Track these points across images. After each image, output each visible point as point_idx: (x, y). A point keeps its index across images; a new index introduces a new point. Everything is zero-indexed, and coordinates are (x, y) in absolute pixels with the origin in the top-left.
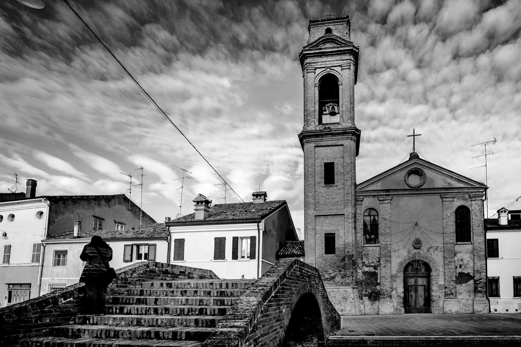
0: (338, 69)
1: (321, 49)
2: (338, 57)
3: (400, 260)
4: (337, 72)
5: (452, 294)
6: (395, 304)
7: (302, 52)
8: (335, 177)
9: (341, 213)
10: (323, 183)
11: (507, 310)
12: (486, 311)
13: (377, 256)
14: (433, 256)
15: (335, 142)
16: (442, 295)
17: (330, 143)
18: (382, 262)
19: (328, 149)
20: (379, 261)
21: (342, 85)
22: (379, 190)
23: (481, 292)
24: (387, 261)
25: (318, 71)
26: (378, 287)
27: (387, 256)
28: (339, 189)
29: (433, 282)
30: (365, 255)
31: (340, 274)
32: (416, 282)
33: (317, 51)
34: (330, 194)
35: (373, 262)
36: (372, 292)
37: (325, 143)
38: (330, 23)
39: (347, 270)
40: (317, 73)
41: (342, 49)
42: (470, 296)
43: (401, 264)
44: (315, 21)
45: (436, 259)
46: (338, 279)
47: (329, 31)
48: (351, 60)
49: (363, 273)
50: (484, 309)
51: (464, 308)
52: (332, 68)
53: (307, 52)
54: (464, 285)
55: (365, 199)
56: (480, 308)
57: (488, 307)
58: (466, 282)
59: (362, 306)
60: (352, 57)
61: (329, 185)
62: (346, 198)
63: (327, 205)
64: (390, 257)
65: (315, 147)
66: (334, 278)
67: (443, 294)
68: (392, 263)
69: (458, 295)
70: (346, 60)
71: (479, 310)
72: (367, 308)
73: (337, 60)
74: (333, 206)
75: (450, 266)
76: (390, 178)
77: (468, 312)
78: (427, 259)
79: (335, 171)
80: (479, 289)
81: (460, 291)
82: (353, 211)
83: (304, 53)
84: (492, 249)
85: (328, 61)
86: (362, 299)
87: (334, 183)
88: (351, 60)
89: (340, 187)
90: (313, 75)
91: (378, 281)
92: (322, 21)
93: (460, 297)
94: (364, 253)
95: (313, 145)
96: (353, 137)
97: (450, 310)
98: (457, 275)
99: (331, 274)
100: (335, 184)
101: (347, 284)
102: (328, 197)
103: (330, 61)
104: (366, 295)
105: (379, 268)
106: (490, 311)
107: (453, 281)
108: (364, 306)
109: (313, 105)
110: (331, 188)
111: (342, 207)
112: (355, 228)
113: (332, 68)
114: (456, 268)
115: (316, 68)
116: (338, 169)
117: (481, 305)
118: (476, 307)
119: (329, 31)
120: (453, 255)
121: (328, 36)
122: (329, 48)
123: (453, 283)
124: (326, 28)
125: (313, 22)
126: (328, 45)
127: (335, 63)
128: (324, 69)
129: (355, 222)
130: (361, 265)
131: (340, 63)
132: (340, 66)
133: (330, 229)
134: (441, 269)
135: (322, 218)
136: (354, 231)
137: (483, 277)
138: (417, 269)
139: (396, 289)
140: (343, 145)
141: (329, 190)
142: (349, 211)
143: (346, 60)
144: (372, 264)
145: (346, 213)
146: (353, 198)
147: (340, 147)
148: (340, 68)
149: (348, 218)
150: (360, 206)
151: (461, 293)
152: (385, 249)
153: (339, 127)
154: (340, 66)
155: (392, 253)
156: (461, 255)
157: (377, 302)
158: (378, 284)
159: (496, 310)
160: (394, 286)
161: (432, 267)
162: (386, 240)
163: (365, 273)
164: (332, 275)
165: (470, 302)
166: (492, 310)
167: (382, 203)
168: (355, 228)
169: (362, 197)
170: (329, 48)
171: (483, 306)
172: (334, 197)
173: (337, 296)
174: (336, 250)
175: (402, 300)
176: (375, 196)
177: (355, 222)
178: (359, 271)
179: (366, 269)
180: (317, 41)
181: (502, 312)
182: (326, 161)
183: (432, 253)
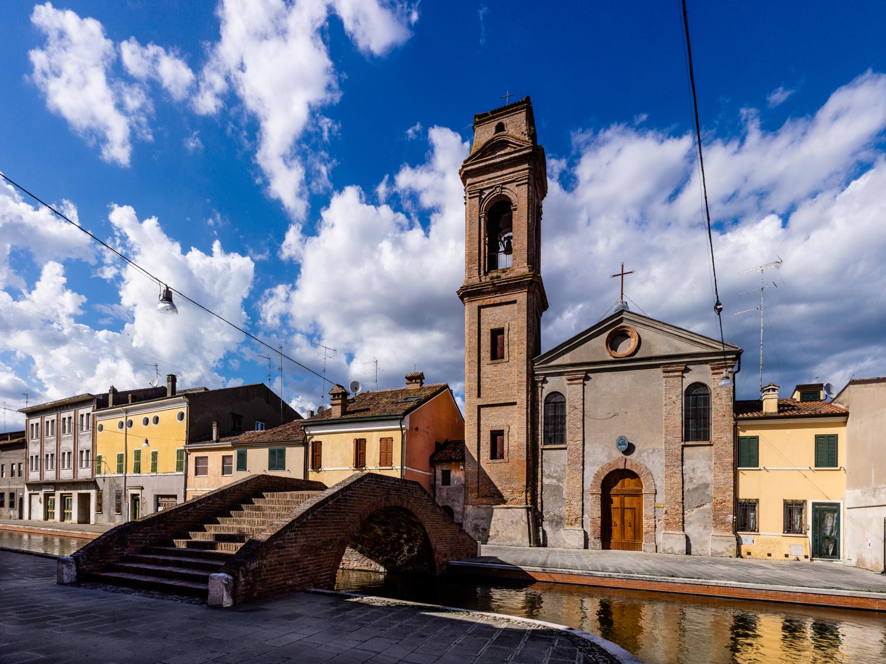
0: (512, 186)
3: (596, 469)
7: (463, 167)
9: (512, 401)
17: (498, 300)
21: (515, 209)
28: (510, 366)
32: (622, 502)
38: (502, 115)
40: (483, 197)
43: (597, 475)
47: (500, 128)
55: (548, 379)
75: (673, 480)
87: (503, 357)
100: (506, 359)
119: (500, 128)
124: (496, 123)
127: (507, 178)
135: (488, 409)
138: (618, 487)
140: (515, 302)
142: (522, 397)
145: (518, 401)
153: (511, 275)
170: (502, 156)
182: (493, 326)
183: (646, 459)
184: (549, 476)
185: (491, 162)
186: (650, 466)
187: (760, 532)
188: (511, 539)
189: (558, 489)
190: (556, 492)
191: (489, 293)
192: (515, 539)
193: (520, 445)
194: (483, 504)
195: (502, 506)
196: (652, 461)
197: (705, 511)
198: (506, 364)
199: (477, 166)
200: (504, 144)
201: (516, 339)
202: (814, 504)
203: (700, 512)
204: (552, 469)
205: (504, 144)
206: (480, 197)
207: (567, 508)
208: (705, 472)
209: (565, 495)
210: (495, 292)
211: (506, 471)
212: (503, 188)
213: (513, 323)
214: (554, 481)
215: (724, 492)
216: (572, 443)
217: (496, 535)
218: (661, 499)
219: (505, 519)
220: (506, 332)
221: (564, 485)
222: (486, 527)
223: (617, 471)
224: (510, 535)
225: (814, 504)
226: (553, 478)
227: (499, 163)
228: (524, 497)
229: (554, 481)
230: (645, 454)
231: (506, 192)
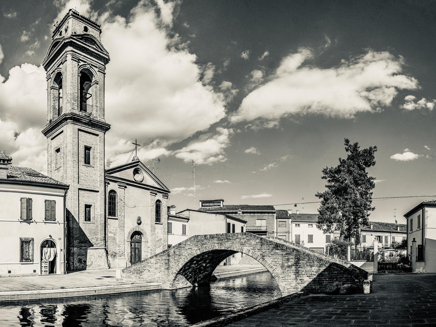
0: (97, 70)
35: (113, 230)
127: (94, 63)
184: (111, 232)
186: (145, 230)
188: (99, 266)
189: (114, 239)
190: (114, 240)
191: (85, 124)
192: (101, 266)
194: (82, 247)
195: (91, 248)
196: (145, 228)
206: (78, 65)
207: (118, 248)
209: (117, 242)
210: (89, 125)
211: (94, 228)
214: (112, 235)
217: (91, 264)
219: (95, 255)
221: (117, 237)
222: (85, 260)
223: (136, 231)
224: (99, 263)
226: (112, 233)
227: (91, 51)
228: (103, 243)
229: (112, 235)
230: (144, 225)
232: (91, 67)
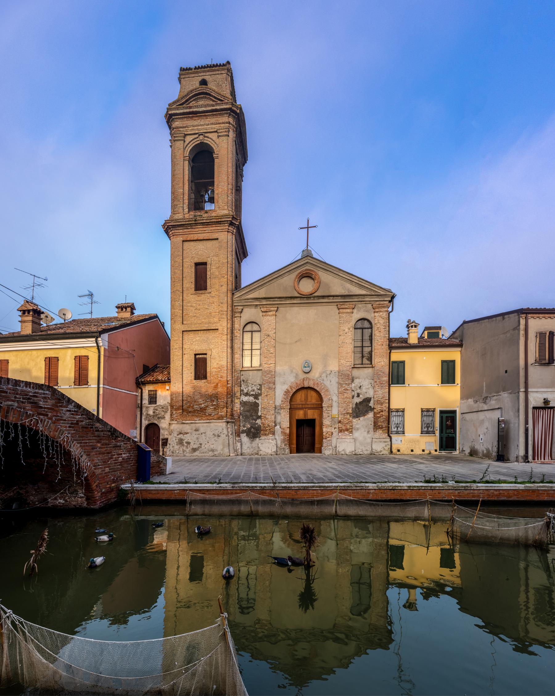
0: (214, 136)
1: (190, 107)
2: (213, 120)
4: (213, 140)
5: (347, 430)
6: (279, 442)
8: (208, 281)
10: (193, 289)
11: (412, 451)
12: (386, 452)
13: (259, 382)
14: (325, 383)
15: (208, 234)
16: (335, 432)
17: (201, 236)
18: (263, 390)
19: (200, 246)
20: (260, 389)
21: (217, 158)
22: (262, 299)
23: (382, 428)
24: (270, 388)
25: (189, 139)
26: (259, 421)
27: (270, 383)
29: (325, 415)
30: (243, 381)
31: (213, 405)
33: (185, 111)
34: (201, 303)
35: (254, 390)
36: (252, 427)
37: (196, 237)
39: (220, 399)
41: (218, 107)
42: (368, 432)
43: (287, 392)
44: (187, 69)
45: (329, 386)
46: (210, 410)
47: (204, 82)
48: (229, 123)
49: (241, 403)
50: (384, 449)
51: (361, 448)
52: (206, 135)
53: (173, 112)
54: (361, 418)
56: (380, 446)
57: (389, 447)
58: (364, 415)
59: (239, 445)
60: (231, 120)
61: (201, 292)
62: (221, 309)
63: (197, 317)
64: (274, 384)
65: (183, 241)
66: (205, 410)
67: (337, 430)
68: (276, 391)
69: (354, 431)
70: (223, 123)
71: (379, 450)
72: (245, 447)
73: (212, 124)
74: (205, 319)
75: (346, 395)
76: (275, 284)
77: (366, 452)
78: (318, 387)
79: (208, 273)
80: (380, 424)
81: (357, 426)
82: (229, 326)
83: (170, 112)
84: (397, 375)
85: (201, 125)
86: (239, 436)
87: (206, 289)
88: (229, 123)
89: (213, 294)
90: (182, 145)
91: (259, 414)
92: (196, 68)
93: (356, 434)
94: (242, 378)
95: (181, 239)
96: (230, 228)
97: (343, 450)
98: (354, 406)
99: (201, 404)
100: (209, 290)
101: (220, 418)
102: (199, 307)
103: (203, 125)
104: (243, 432)
105: (260, 398)
106: (391, 452)
107: (347, 413)
108: (241, 445)
109: (181, 185)
110: (203, 296)
111: (216, 320)
112: (232, 348)
113: (206, 135)
114: (353, 397)
115: (186, 135)
116: (212, 271)
117: (381, 444)
118: (374, 447)
119: (204, 82)
120: (350, 381)
121: (203, 89)
122: (201, 106)
123: (348, 416)
125: (184, 70)
126: (201, 102)
128: (197, 136)
129: (232, 340)
130: (238, 394)
131: (217, 127)
132: (216, 132)
133: (199, 348)
134: (335, 398)
136: (229, 350)
137: (385, 408)
139: (280, 423)
140: (217, 239)
141: (199, 298)
143: (223, 123)
144: (252, 393)
146: (230, 309)
147: (215, 242)
148: (216, 134)
149: (222, 334)
150: (239, 319)
151: (358, 429)
152: (268, 374)
154: (216, 132)
155: (277, 379)
156: (360, 380)
157: (258, 439)
158: (260, 417)
159: (399, 451)
160: (279, 419)
161: (323, 396)
162: (269, 363)
163: (243, 404)
164: (203, 405)
165: (369, 440)
166: (394, 451)
167: (265, 315)
168: (232, 348)
169: (242, 308)
171: (383, 445)
172: (206, 307)
173: (208, 433)
174: (208, 375)
175: (287, 438)
176: (257, 305)
177: (232, 340)
178: (237, 401)
179: (245, 399)
180: (186, 96)
181: (406, 453)
182: (197, 260)
183: (325, 379)
184: (247, 394)
185: (194, 110)
187: (406, 434)
193: (220, 368)
197: (368, 419)
198: (209, 295)
199: (182, 111)
200: (206, 95)
201: (217, 273)
202: (442, 412)
203: (364, 420)
204: (250, 389)
205: (206, 95)
208: (368, 389)
212: (205, 137)
213: (215, 258)
215: (382, 404)
216: (266, 366)
218: (335, 411)
220: (208, 266)
225: (442, 412)
226: (250, 396)
231: (207, 141)
232: (205, 137)
